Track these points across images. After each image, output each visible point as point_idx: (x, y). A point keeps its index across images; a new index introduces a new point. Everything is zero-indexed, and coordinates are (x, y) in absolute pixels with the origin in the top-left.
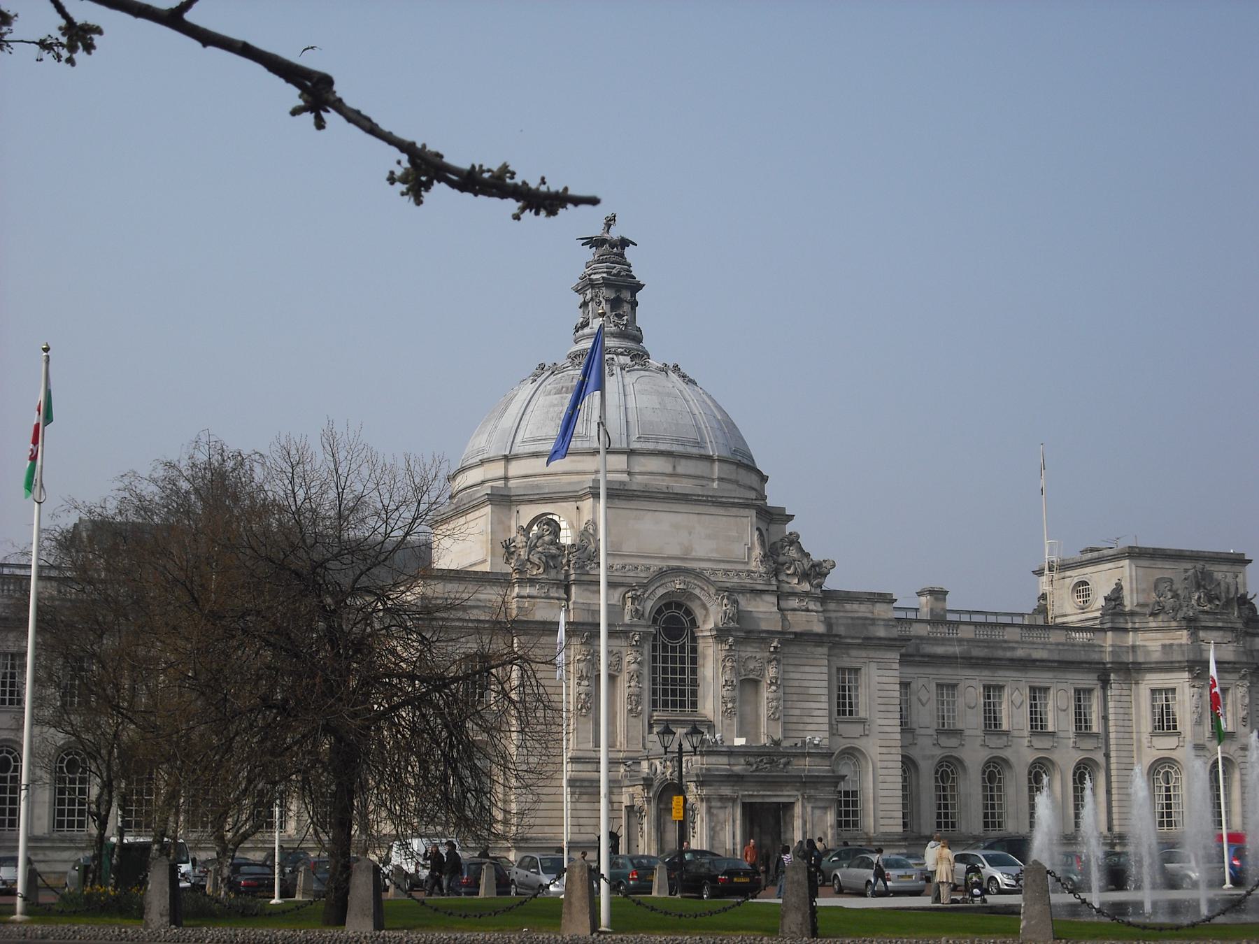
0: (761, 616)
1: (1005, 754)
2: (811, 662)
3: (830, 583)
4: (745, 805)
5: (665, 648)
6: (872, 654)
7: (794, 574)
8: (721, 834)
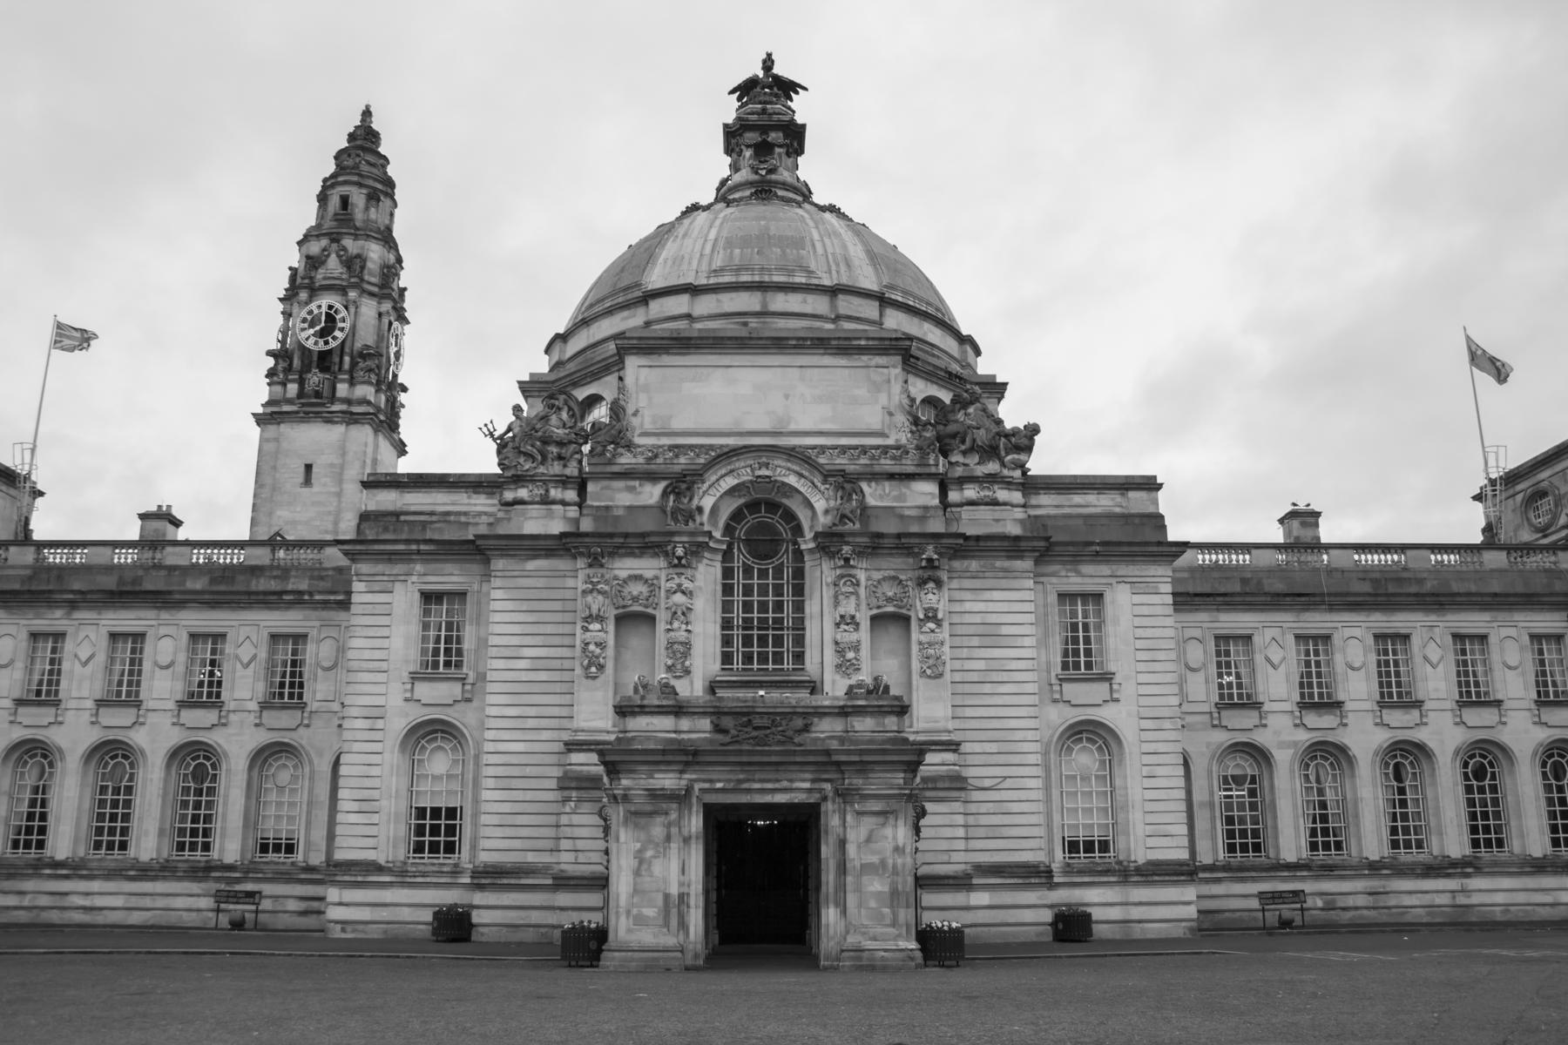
0: (907, 512)
1: (1420, 735)
2: (1004, 583)
3: (1040, 463)
4: (710, 811)
5: (748, 571)
6: (1123, 570)
7: (971, 450)
8: (657, 868)
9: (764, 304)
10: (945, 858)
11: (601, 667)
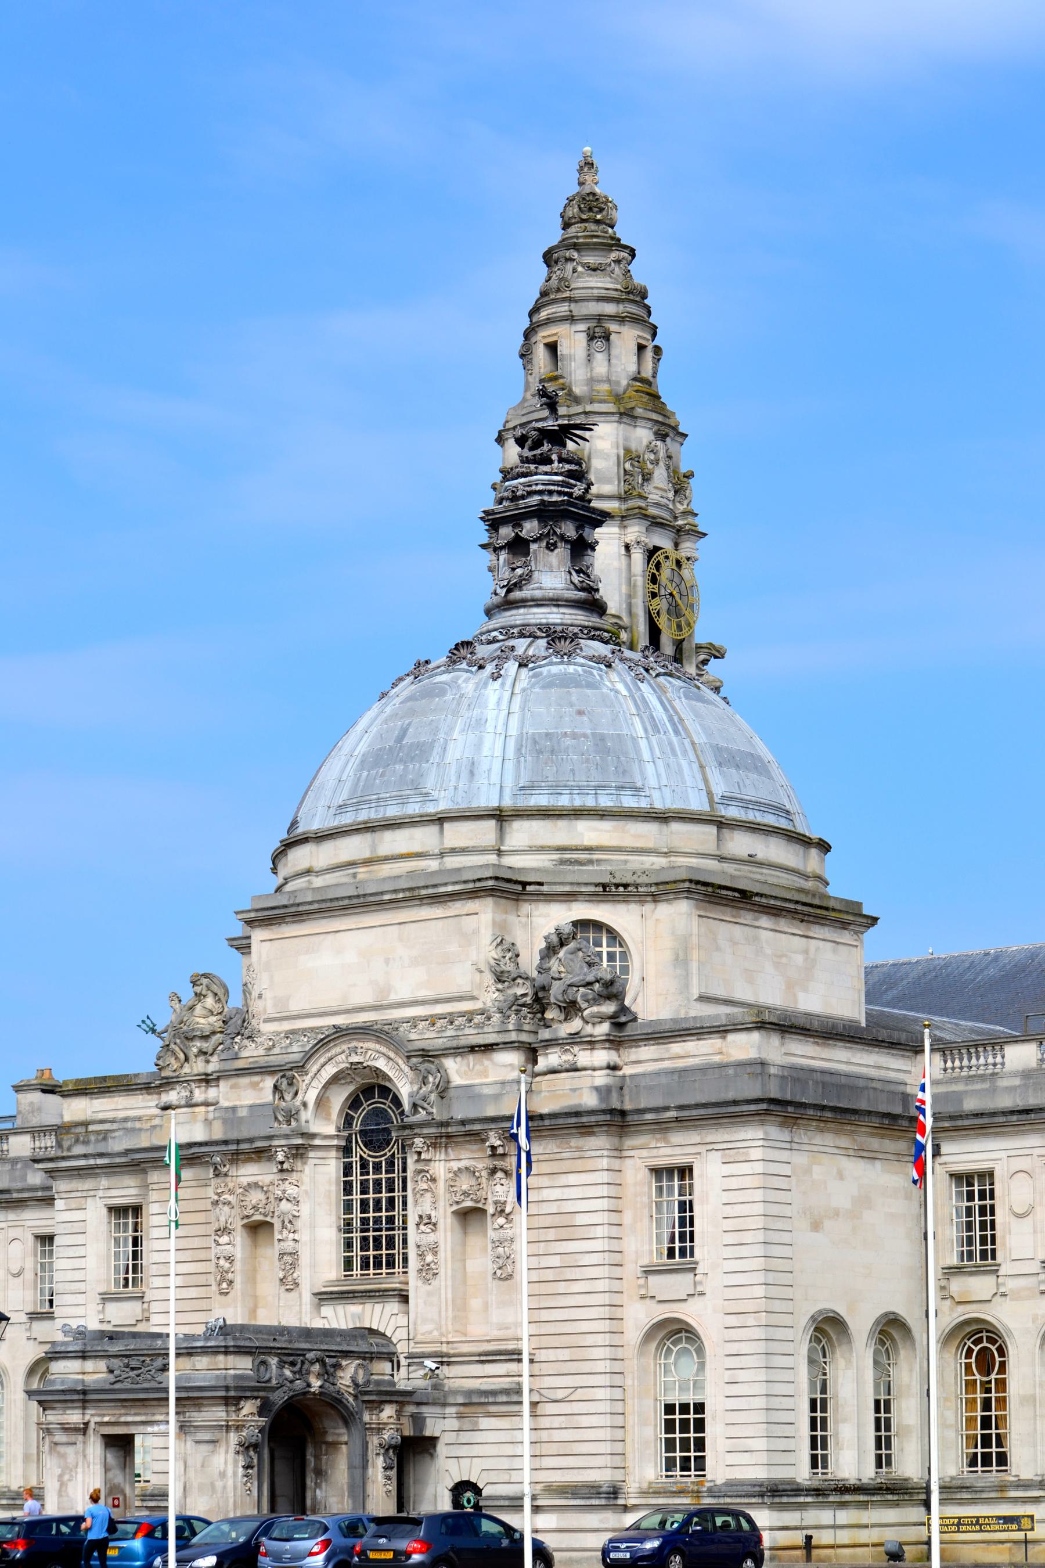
0: (486, 1091)
2: (579, 1165)
5: (364, 1165)
9: (374, 847)
10: (505, 1477)
11: (231, 1283)
